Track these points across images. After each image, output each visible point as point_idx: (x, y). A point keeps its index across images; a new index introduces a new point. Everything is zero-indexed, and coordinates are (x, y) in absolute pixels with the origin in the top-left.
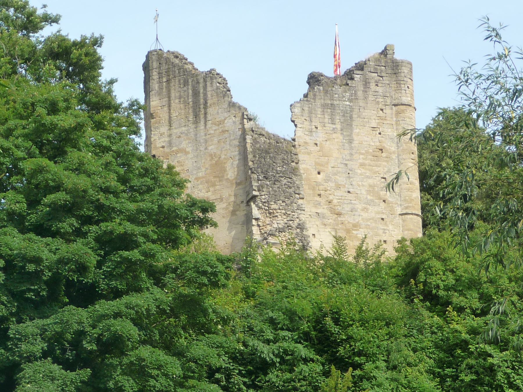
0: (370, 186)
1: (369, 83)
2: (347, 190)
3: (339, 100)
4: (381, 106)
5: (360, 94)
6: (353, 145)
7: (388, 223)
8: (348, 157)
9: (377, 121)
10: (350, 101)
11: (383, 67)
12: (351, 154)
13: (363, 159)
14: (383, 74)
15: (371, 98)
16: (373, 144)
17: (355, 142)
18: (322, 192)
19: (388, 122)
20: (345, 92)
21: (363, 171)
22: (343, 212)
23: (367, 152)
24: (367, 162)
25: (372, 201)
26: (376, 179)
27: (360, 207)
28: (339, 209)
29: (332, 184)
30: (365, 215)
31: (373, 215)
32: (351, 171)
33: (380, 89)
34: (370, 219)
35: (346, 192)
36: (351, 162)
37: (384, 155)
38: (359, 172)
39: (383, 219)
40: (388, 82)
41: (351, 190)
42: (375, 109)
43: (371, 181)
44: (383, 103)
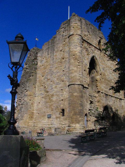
13: (57, 65)
18: (43, 84)
21: (56, 70)
29: (46, 80)
30: (55, 89)
33: (64, 34)
38: (55, 71)
43: (59, 74)
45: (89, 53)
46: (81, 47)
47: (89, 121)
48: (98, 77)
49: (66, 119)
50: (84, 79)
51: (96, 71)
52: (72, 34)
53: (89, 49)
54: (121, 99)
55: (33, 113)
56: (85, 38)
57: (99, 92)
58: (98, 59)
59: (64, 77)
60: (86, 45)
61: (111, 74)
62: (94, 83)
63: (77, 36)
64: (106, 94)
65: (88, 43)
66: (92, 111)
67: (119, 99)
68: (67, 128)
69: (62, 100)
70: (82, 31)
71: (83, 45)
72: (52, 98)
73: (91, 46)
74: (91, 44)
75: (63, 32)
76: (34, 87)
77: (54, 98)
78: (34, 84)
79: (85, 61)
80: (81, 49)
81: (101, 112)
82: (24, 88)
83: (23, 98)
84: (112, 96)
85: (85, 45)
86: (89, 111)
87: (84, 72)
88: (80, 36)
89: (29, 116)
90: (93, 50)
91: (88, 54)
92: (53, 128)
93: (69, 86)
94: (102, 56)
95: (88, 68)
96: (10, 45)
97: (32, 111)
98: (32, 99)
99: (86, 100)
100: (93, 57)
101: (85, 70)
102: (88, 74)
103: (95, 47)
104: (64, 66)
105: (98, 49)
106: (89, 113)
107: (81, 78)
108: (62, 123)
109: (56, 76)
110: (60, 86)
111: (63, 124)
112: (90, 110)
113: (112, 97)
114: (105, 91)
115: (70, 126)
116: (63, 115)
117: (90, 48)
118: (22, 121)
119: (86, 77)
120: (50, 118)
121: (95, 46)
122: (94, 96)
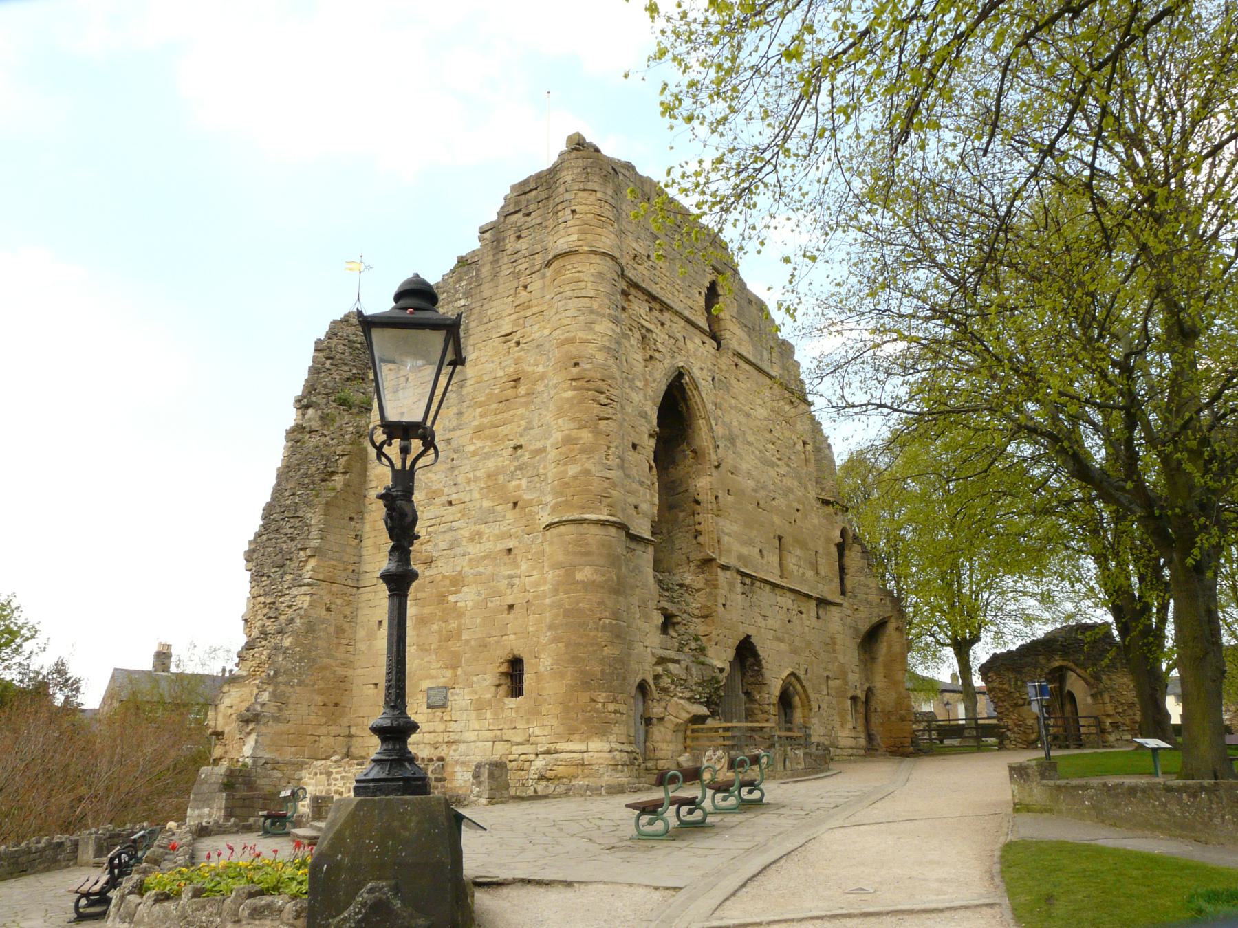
0: (489, 476)
1: (504, 239)
2: (444, 499)
3: (448, 303)
4: (523, 280)
5: (486, 271)
6: (465, 391)
7: (519, 559)
8: (454, 423)
9: (514, 317)
10: (467, 295)
11: (534, 193)
12: (460, 413)
14: (532, 207)
15: (505, 271)
16: (501, 373)
17: (469, 382)
19: (535, 310)
20: (461, 279)
21: (479, 444)
22: (435, 554)
23: (490, 397)
24: (486, 420)
25: (491, 510)
26: (500, 456)
27: (467, 534)
28: (429, 548)
30: (475, 550)
31: (490, 545)
32: (456, 451)
33: (523, 245)
34: (484, 558)
35: (443, 505)
36: (458, 433)
37: (522, 390)
38: (471, 448)
39: (510, 550)
40: (538, 221)
41: (453, 497)
42: (512, 292)
43: (491, 464)
44: (528, 272)
45: (657, 355)
46: (615, 321)
47: (655, 721)
48: (703, 484)
49: (535, 712)
50: (631, 492)
51: (694, 451)
52: (566, 248)
53: (659, 334)
54: (822, 602)
55: (344, 679)
56: (639, 273)
57: (708, 562)
58: (705, 385)
59: (524, 482)
60: (642, 312)
61: (773, 465)
62: (681, 515)
63: (597, 259)
64: (743, 574)
65: (653, 298)
66: (671, 666)
67: (814, 603)
68: (539, 763)
69: (511, 607)
70: (621, 233)
71: (624, 309)
72: (452, 598)
73: (667, 316)
74: (665, 307)
75: (519, 237)
76: (353, 534)
77: (467, 598)
78: (351, 519)
79: (636, 397)
80: (618, 330)
81: (721, 670)
82: (292, 540)
83: (287, 598)
84: (774, 586)
85: (639, 307)
86: (659, 669)
87: (631, 455)
88: (613, 258)
89: (319, 699)
90: (680, 336)
91: (651, 357)
92: (457, 762)
93: (548, 527)
94: (724, 368)
95: (651, 436)
96: (376, 334)
97: (341, 672)
98: (339, 602)
99: (643, 606)
100: (680, 375)
101: (634, 446)
102: (651, 468)
103: (688, 321)
104: (523, 423)
105: (702, 331)
106: (657, 677)
107: (614, 485)
108: (509, 734)
109: (478, 474)
110: (497, 532)
111: (519, 740)
112: (661, 661)
113: (778, 591)
114: (741, 557)
115: (556, 752)
116: (517, 691)
117: (663, 324)
118: (274, 727)
119: (641, 484)
120: (444, 706)
121: (686, 313)
122: (681, 585)
